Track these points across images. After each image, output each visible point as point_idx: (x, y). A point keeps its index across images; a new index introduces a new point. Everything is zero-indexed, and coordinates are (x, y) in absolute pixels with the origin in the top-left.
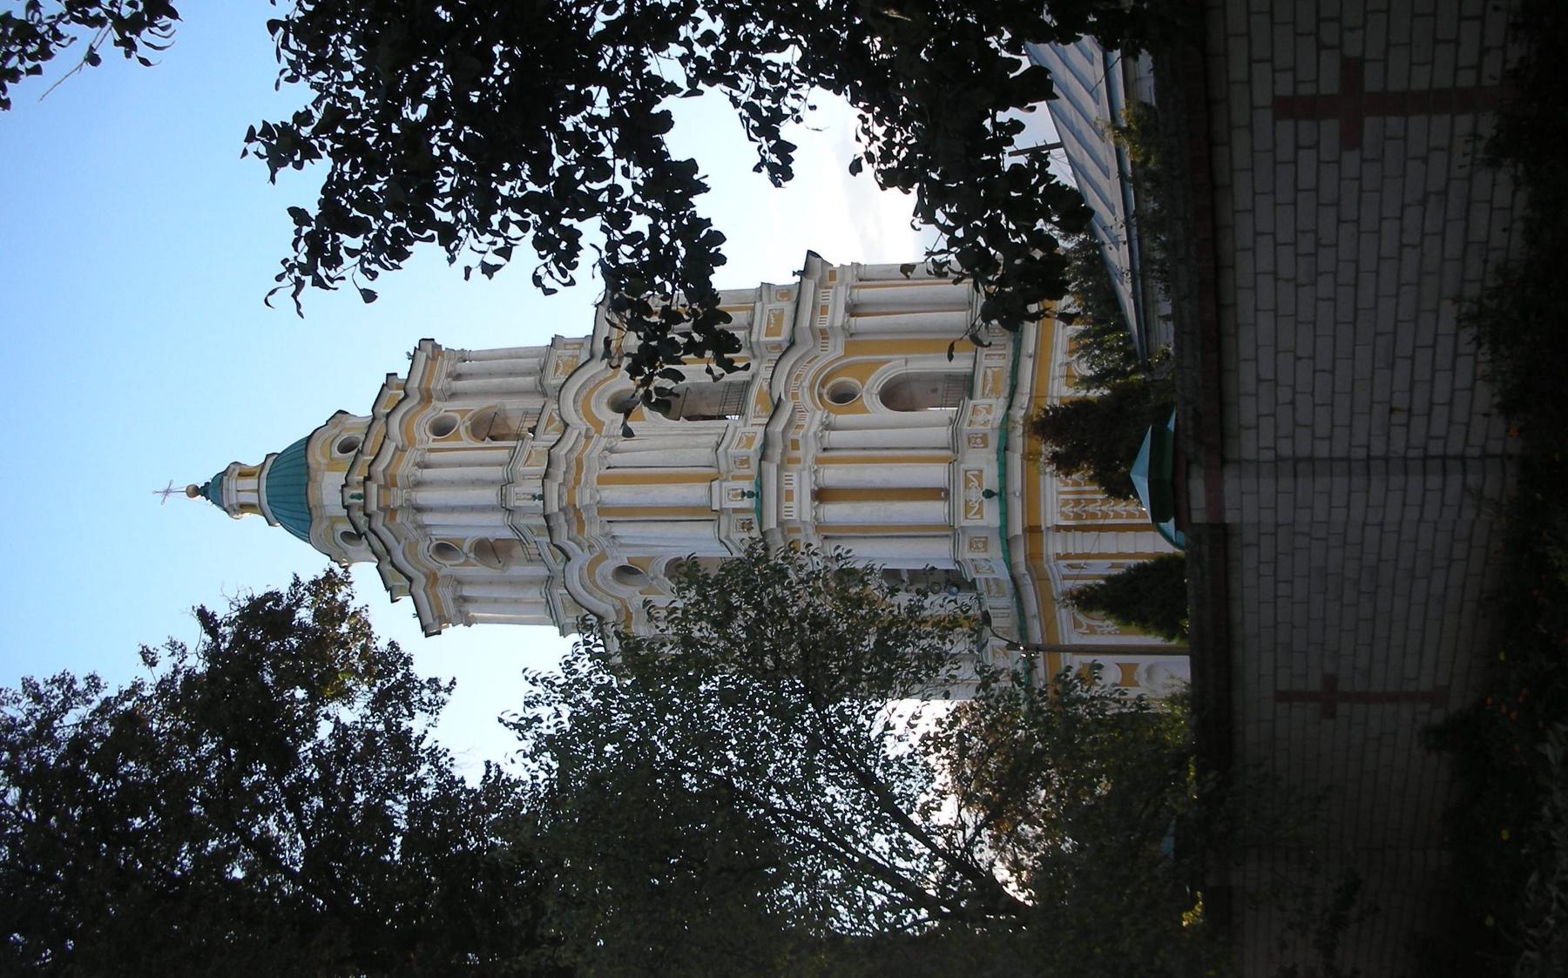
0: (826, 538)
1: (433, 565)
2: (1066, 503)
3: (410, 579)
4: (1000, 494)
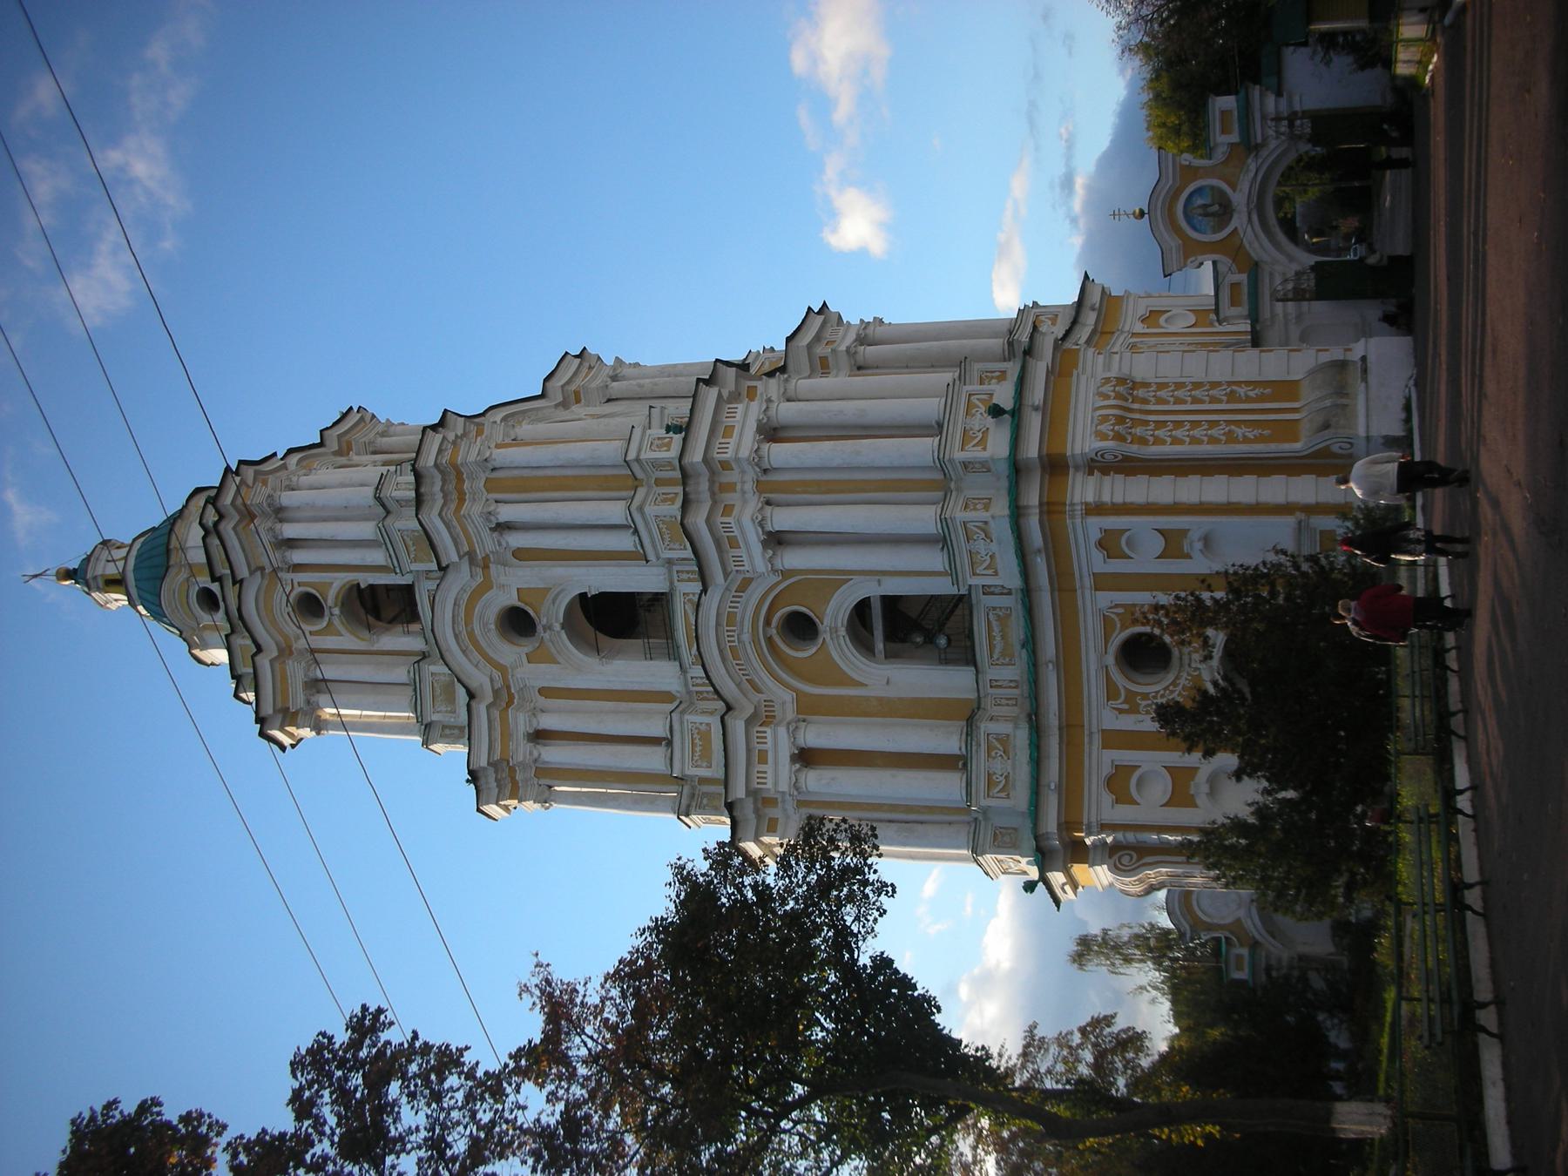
0: (768, 503)
2: (1105, 419)
4: (1014, 416)
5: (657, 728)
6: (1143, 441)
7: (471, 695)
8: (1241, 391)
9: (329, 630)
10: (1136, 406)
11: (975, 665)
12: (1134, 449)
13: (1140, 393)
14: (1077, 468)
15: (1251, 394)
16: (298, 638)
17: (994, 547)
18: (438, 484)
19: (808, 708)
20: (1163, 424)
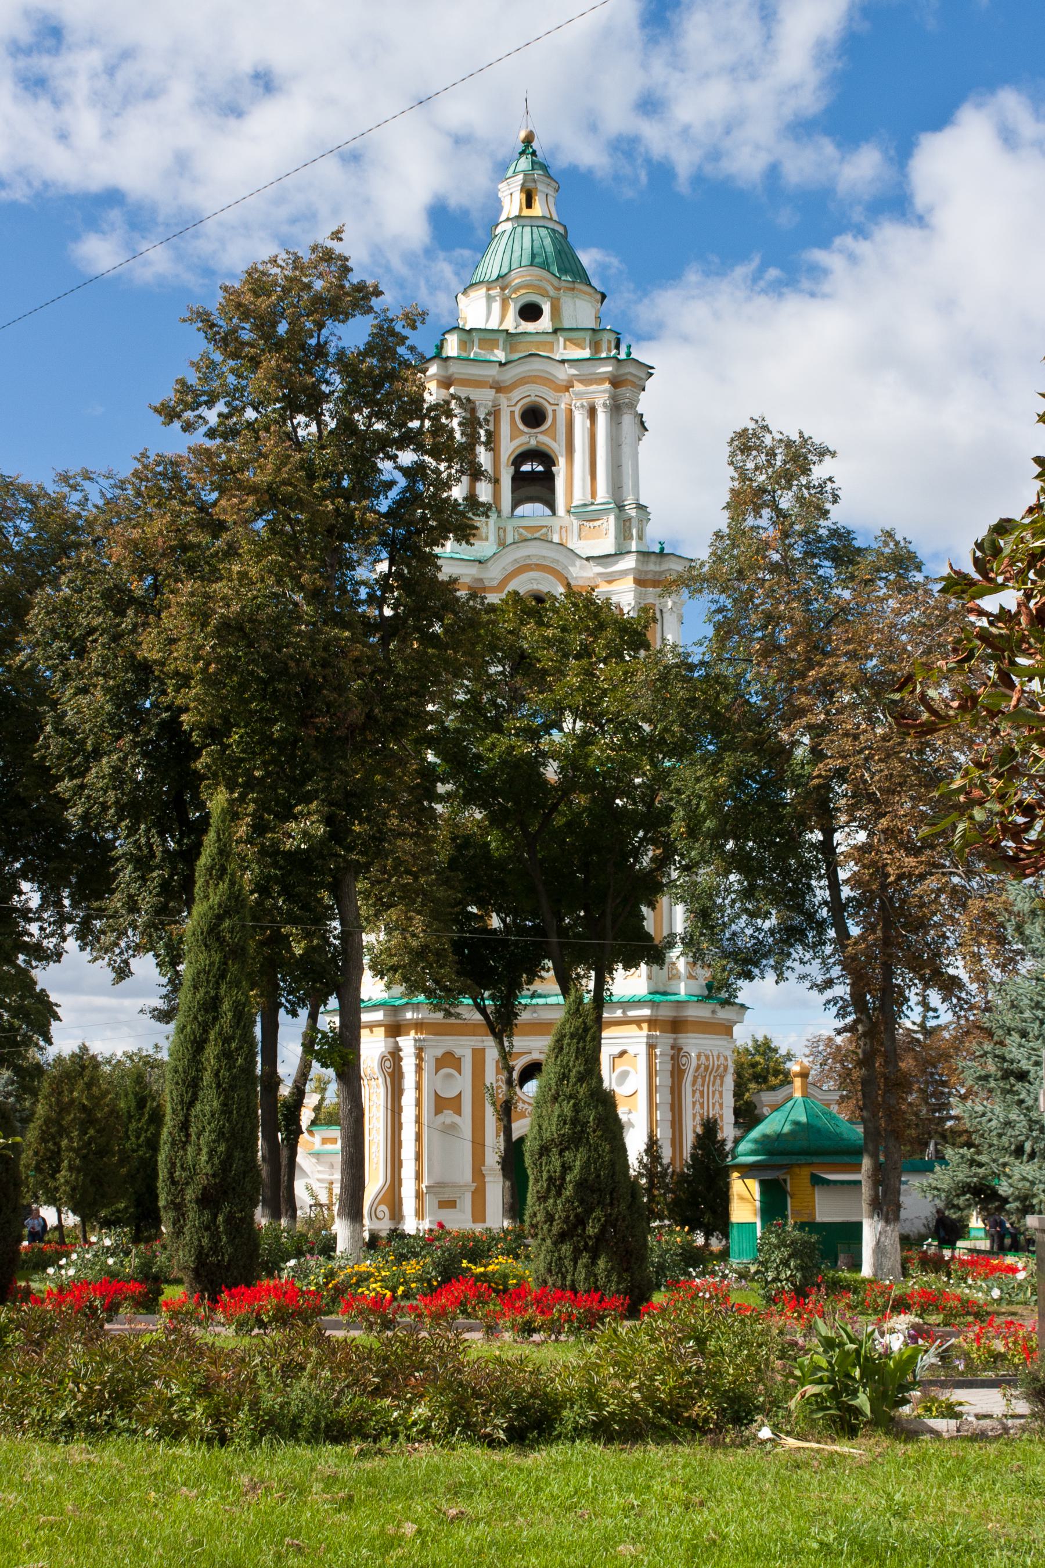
1: (516, 394)
3: (501, 364)
6: (694, 1083)
9: (515, 434)
12: (688, 1079)
13: (718, 1081)
16: (509, 399)
18: (657, 569)
20: (702, 1096)
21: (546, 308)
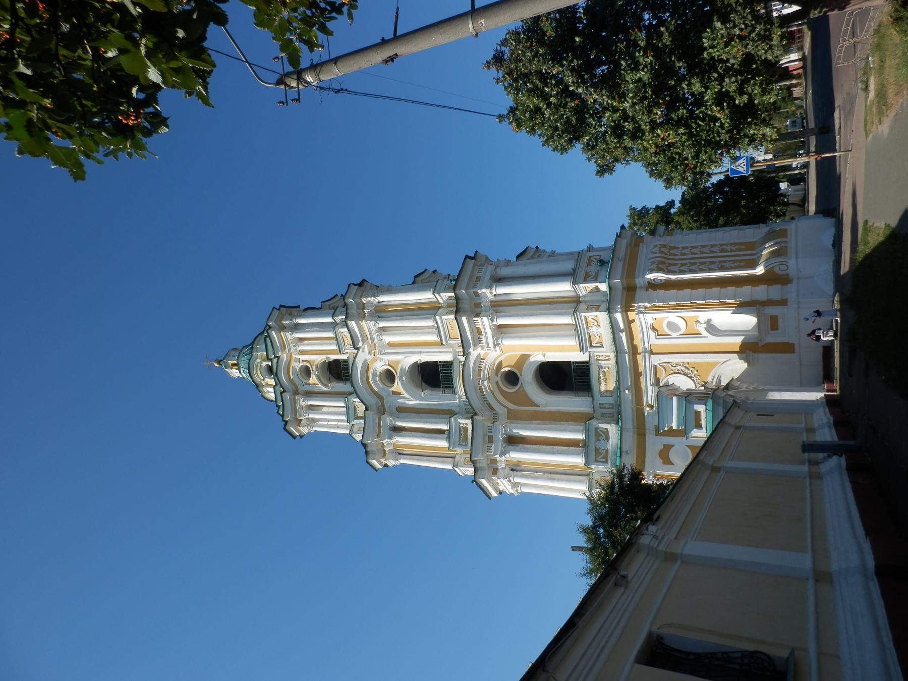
2: (653, 263)
5: (445, 427)
6: (674, 273)
7: (367, 409)
8: (728, 248)
10: (671, 257)
11: (592, 396)
14: (641, 288)
15: (734, 248)
17: (601, 330)
19: (513, 417)
21: (265, 364)
